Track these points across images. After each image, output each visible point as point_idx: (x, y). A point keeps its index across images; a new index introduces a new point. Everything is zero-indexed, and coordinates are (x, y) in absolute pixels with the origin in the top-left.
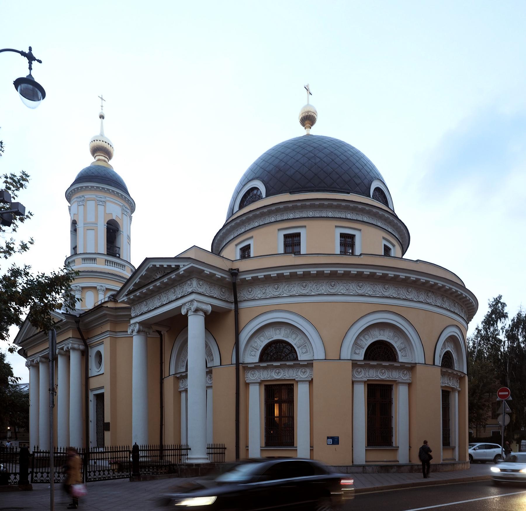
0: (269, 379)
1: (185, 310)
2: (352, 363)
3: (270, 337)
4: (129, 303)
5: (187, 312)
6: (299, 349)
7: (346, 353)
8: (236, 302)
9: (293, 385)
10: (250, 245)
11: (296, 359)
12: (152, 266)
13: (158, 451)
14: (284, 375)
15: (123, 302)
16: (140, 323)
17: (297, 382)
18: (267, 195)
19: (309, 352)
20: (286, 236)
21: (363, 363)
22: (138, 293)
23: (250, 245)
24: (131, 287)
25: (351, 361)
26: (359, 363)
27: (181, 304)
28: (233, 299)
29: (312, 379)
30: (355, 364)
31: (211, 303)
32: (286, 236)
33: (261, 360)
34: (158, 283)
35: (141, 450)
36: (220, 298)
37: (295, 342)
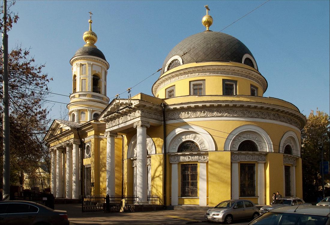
2: (231, 153)
4: (105, 122)
5: (137, 126)
8: (164, 121)
21: (237, 152)
26: (235, 152)
28: (162, 118)
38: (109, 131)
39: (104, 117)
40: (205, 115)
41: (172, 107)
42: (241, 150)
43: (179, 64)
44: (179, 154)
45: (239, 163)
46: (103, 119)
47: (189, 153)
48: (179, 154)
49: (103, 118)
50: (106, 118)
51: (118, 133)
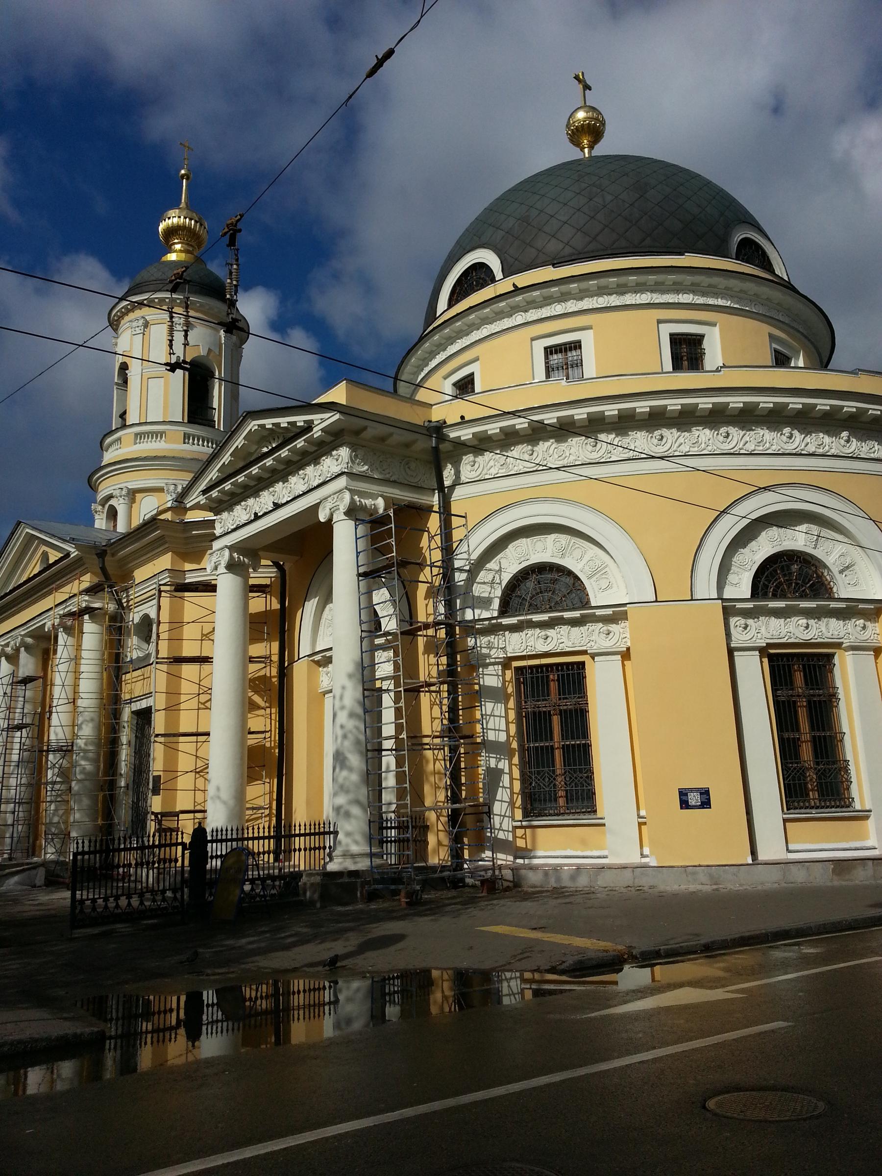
0: (524, 653)
1: (327, 512)
2: (724, 608)
3: (523, 559)
4: (211, 510)
5: (332, 515)
6: (592, 580)
7: (706, 586)
9: (583, 663)
10: (473, 374)
11: (585, 603)
12: (256, 427)
13: (272, 840)
14: (560, 641)
15: (197, 507)
16: (232, 548)
17: (593, 656)
18: (507, 273)
19: (615, 585)
20: (549, 351)
21: (750, 605)
22: (227, 486)
23: (473, 374)
24: (213, 474)
25: (720, 601)
26: (739, 605)
27: (319, 501)
29: (628, 649)
30: (729, 610)
31: (385, 494)
32: (549, 351)
33: (504, 611)
34: (269, 461)
35: (212, 841)
36: (406, 482)
37: (580, 566)
38: (226, 546)
39: (204, 492)
40: (600, 454)
41: (466, 434)
42: (765, 597)
43: (493, 280)
44: (505, 621)
45: (763, 651)
46: (202, 500)
47: (544, 617)
48: (505, 621)
49: (201, 497)
50: (214, 493)
51: (261, 553)
